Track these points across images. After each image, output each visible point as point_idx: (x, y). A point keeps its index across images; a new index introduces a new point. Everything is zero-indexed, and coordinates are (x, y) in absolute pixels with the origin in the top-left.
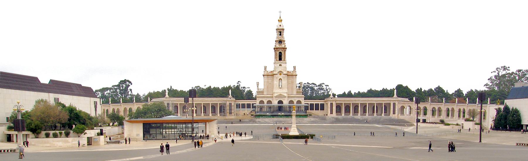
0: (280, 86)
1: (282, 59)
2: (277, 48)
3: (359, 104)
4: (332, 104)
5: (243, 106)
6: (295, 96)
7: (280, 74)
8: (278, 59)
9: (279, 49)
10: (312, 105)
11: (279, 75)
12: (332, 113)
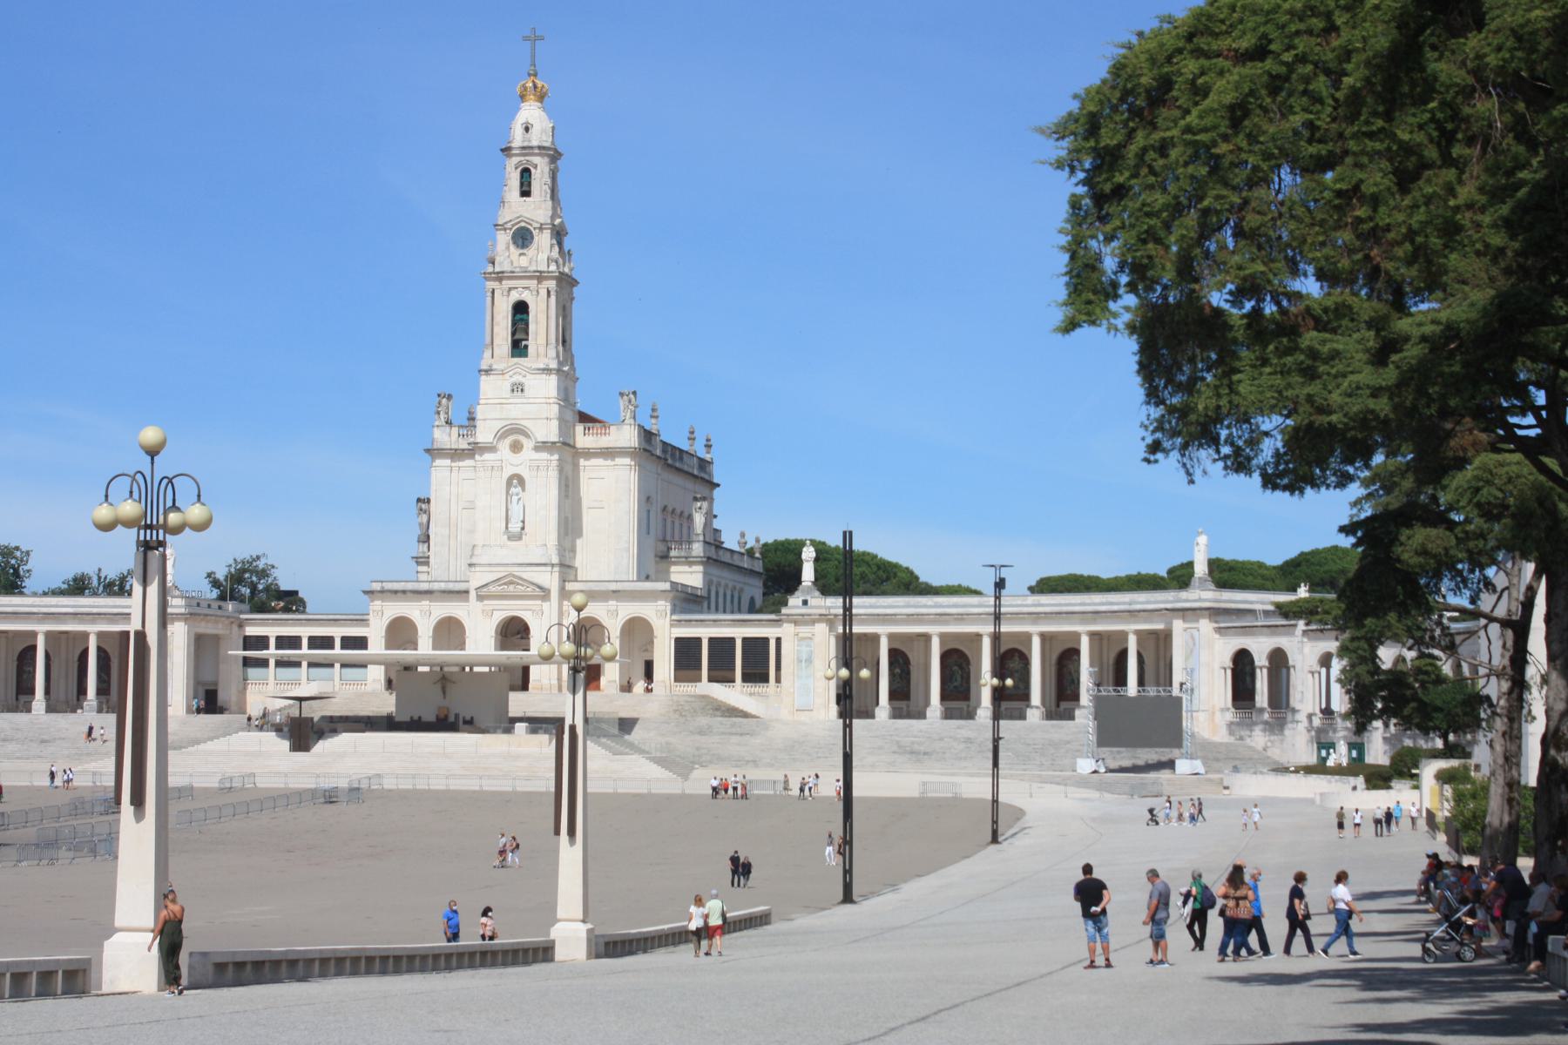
0: (515, 527)
1: (531, 350)
2: (500, 276)
3: (1036, 644)
6: (613, 587)
7: (516, 447)
10: (722, 648)
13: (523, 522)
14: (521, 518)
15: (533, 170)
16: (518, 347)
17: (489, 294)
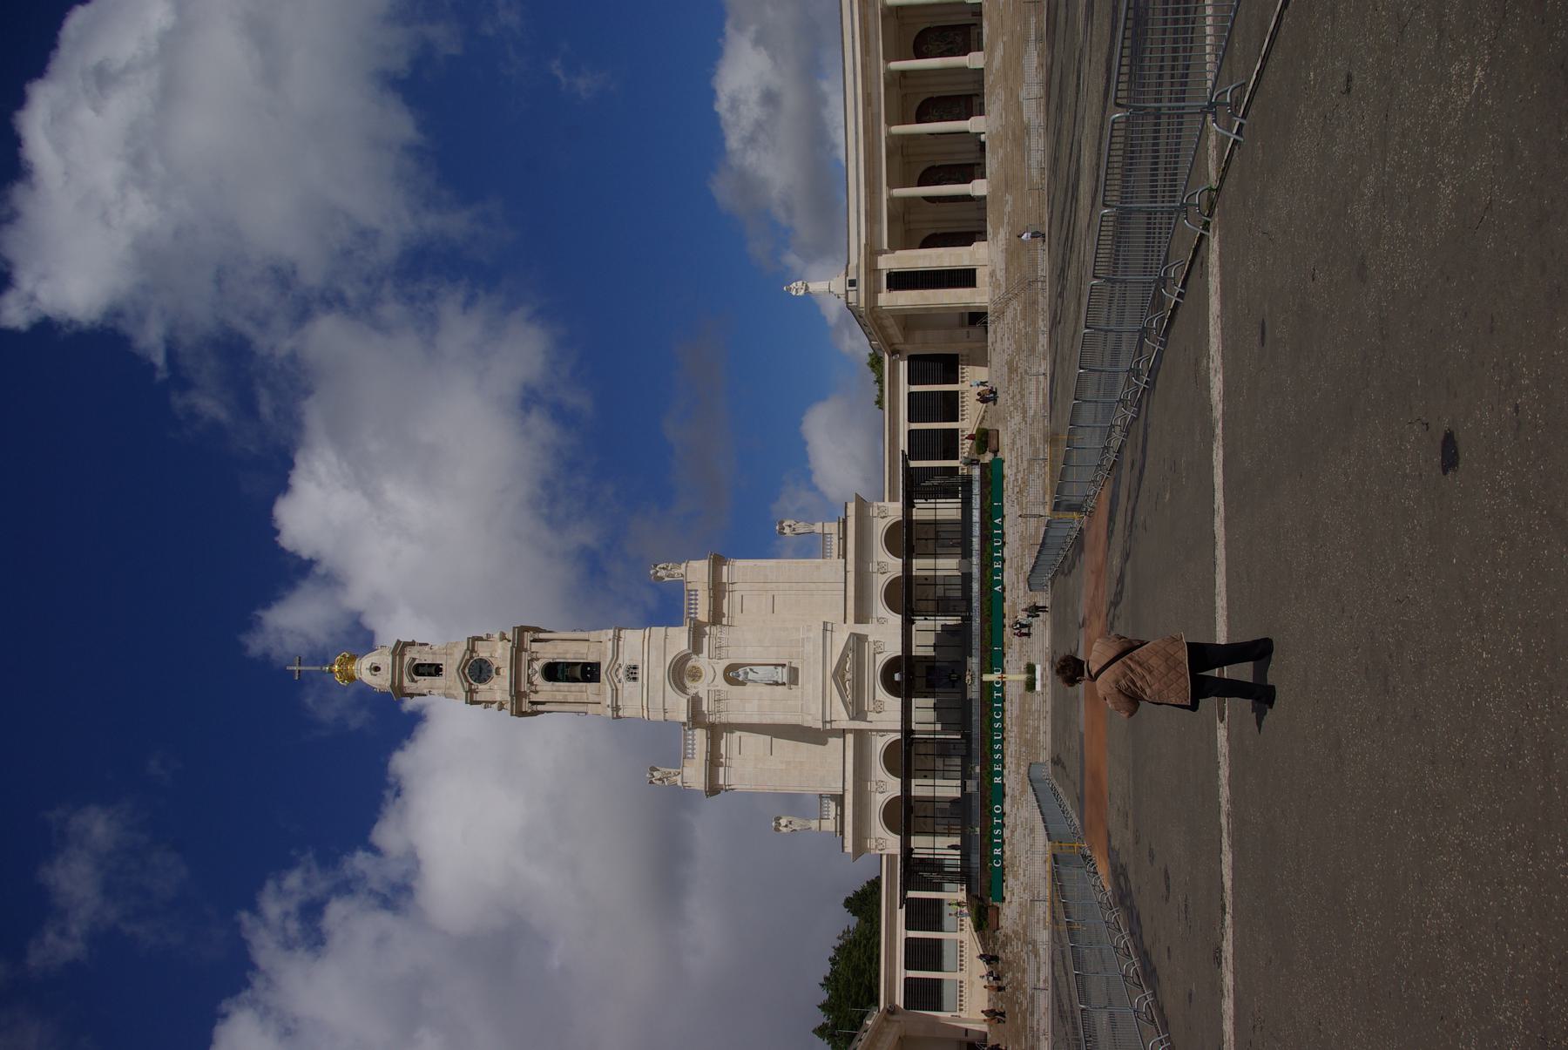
0: (782, 675)
1: (590, 660)
2: (517, 695)
4: (900, 281)
5: (925, 954)
7: (696, 675)
8: (591, 687)
9: (524, 679)
11: (700, 688)
12: (965, 278)
13: (776, 665)
14: (773, 667)
15: (417, 662)
16: (589, 672)
17: (534, 707)
